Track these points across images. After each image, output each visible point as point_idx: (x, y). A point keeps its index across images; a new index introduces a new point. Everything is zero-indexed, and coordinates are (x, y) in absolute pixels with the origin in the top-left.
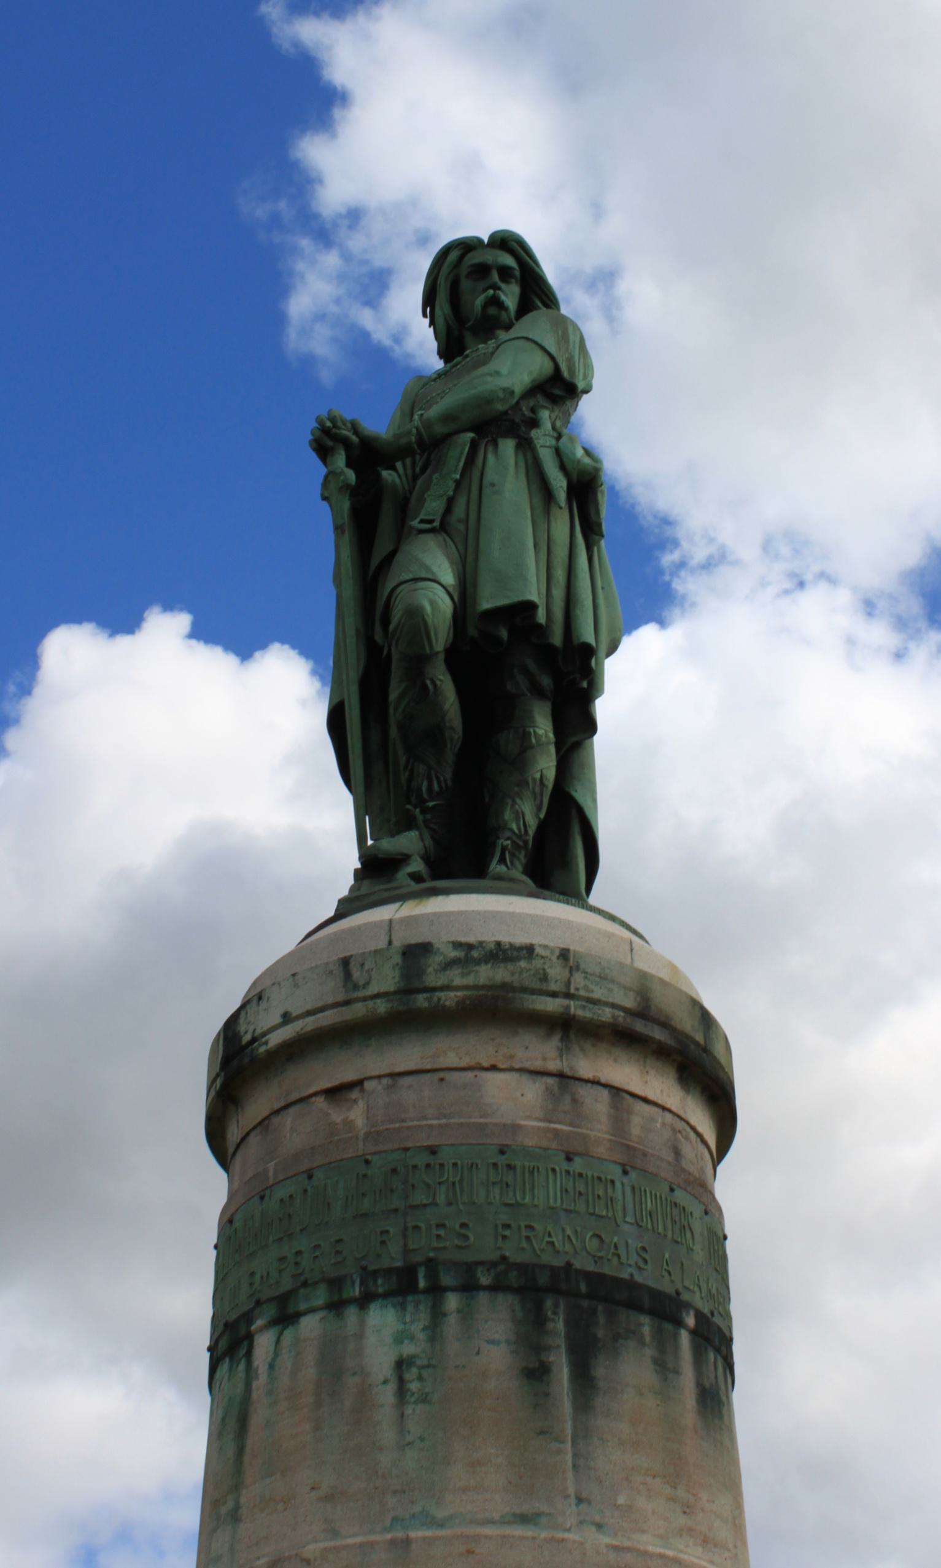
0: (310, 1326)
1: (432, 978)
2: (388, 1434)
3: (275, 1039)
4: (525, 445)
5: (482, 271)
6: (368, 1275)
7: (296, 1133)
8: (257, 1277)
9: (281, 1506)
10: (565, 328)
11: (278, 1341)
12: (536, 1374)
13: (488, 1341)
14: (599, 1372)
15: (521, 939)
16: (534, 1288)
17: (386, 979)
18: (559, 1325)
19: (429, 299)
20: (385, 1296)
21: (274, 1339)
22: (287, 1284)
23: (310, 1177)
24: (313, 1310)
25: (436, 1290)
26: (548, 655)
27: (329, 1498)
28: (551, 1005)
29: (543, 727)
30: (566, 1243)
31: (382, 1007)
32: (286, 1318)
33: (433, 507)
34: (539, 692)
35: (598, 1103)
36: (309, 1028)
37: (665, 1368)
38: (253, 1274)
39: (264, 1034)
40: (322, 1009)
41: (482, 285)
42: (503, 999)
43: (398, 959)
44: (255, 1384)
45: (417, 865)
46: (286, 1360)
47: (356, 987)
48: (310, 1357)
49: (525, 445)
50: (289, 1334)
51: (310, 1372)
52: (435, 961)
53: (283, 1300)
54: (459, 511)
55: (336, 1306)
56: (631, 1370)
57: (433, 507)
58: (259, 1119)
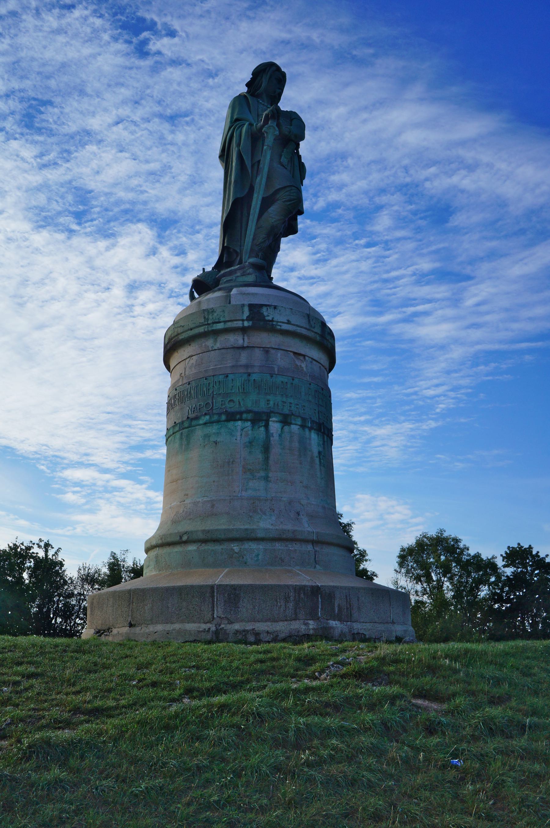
0: (295, 428)
3: (285, 327)
8: (271, 403)
9: (289, 484)
11: (282, 428)
20: (315, 430)
21: (280, 427)
22: (286, 411)
23: (293, 380)
24: (296, 424)
27: (306, 487)
36: (299, 331)
38: (268, 400)
39: (278, 322)
40: (301, 327)
43: (320, 324)
44: (272, 438)
47: (311, 326)
50: (286, 428)
51: (296, 445)
55: (303, 426)
58: (264, 346)
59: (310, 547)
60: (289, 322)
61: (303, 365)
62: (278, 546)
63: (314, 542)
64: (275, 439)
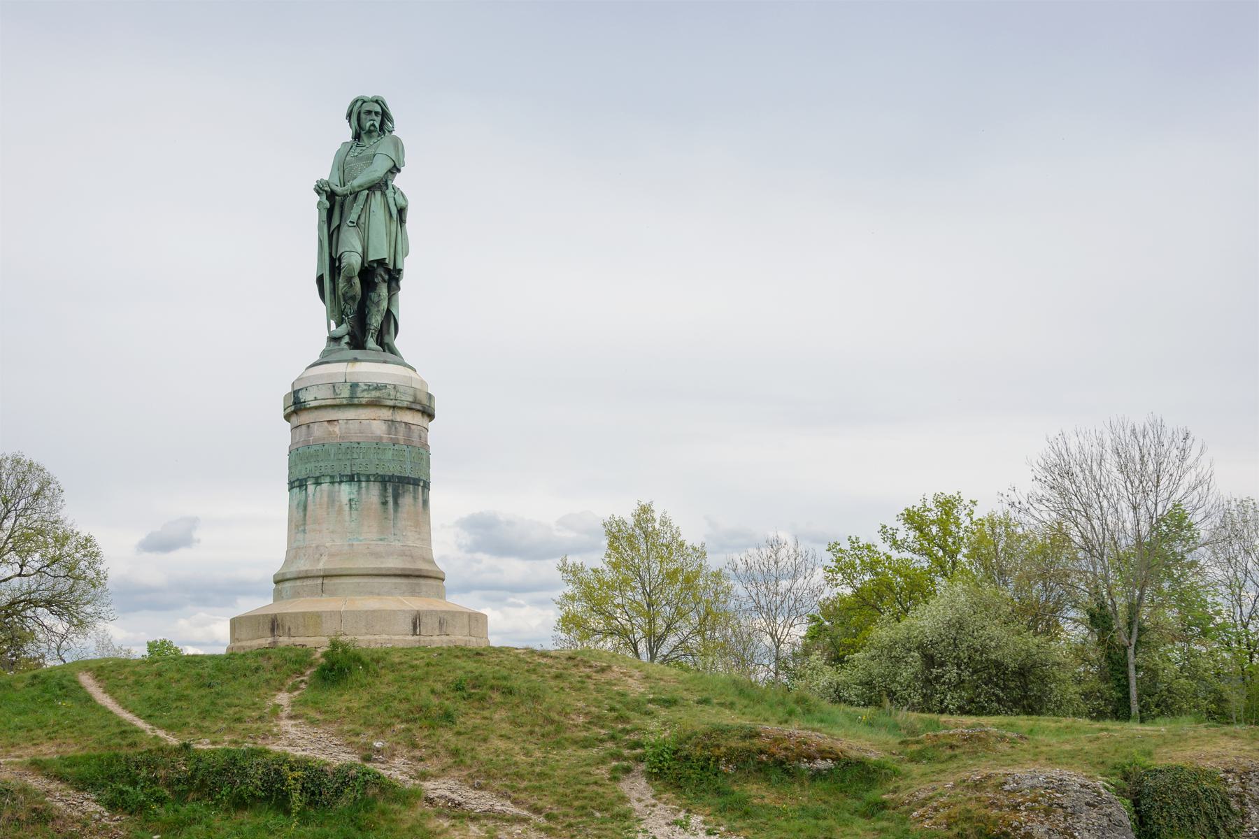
0: (325, 486)
1: (359, 395)
2: (347, 518)
3: (313, 404)
4: (384, 194)
5: (369, 112)
6: (341, 476)
7: (318, 431)
10: (397, 144)
12: (385, 503)
13: (373, 493)
14: (401, 501)
15: (382, 381)
16: (384, 480)
17: (346, 393)
18: (390, 490)
19: (349, 115)
25: (359, 481)
26: (388, 271)
28: (391, 403)
29: (383, 290)
30: (393, 469)
31: (345, 402)
32: (317, 483)
33: (354, 217)
34: (384, 281)
35: (402, 429)
37: (415, 498)
41: (369, 117)
42: (375, 399)
45: (347, 339)
46: (318, 494)
48: (325, 495)
49: (384, 194)
51: (326, 499)
52: (359, 390)
53: (317, 478)
54: (362, 220)
55: (332, 483)
56: (406, 500)
57: (354, 217)
59: (320, 581)
60: (316, 399)
61: (337, 429)
62: (298, 583)
63: (323, 577)
64: (310, 498)
